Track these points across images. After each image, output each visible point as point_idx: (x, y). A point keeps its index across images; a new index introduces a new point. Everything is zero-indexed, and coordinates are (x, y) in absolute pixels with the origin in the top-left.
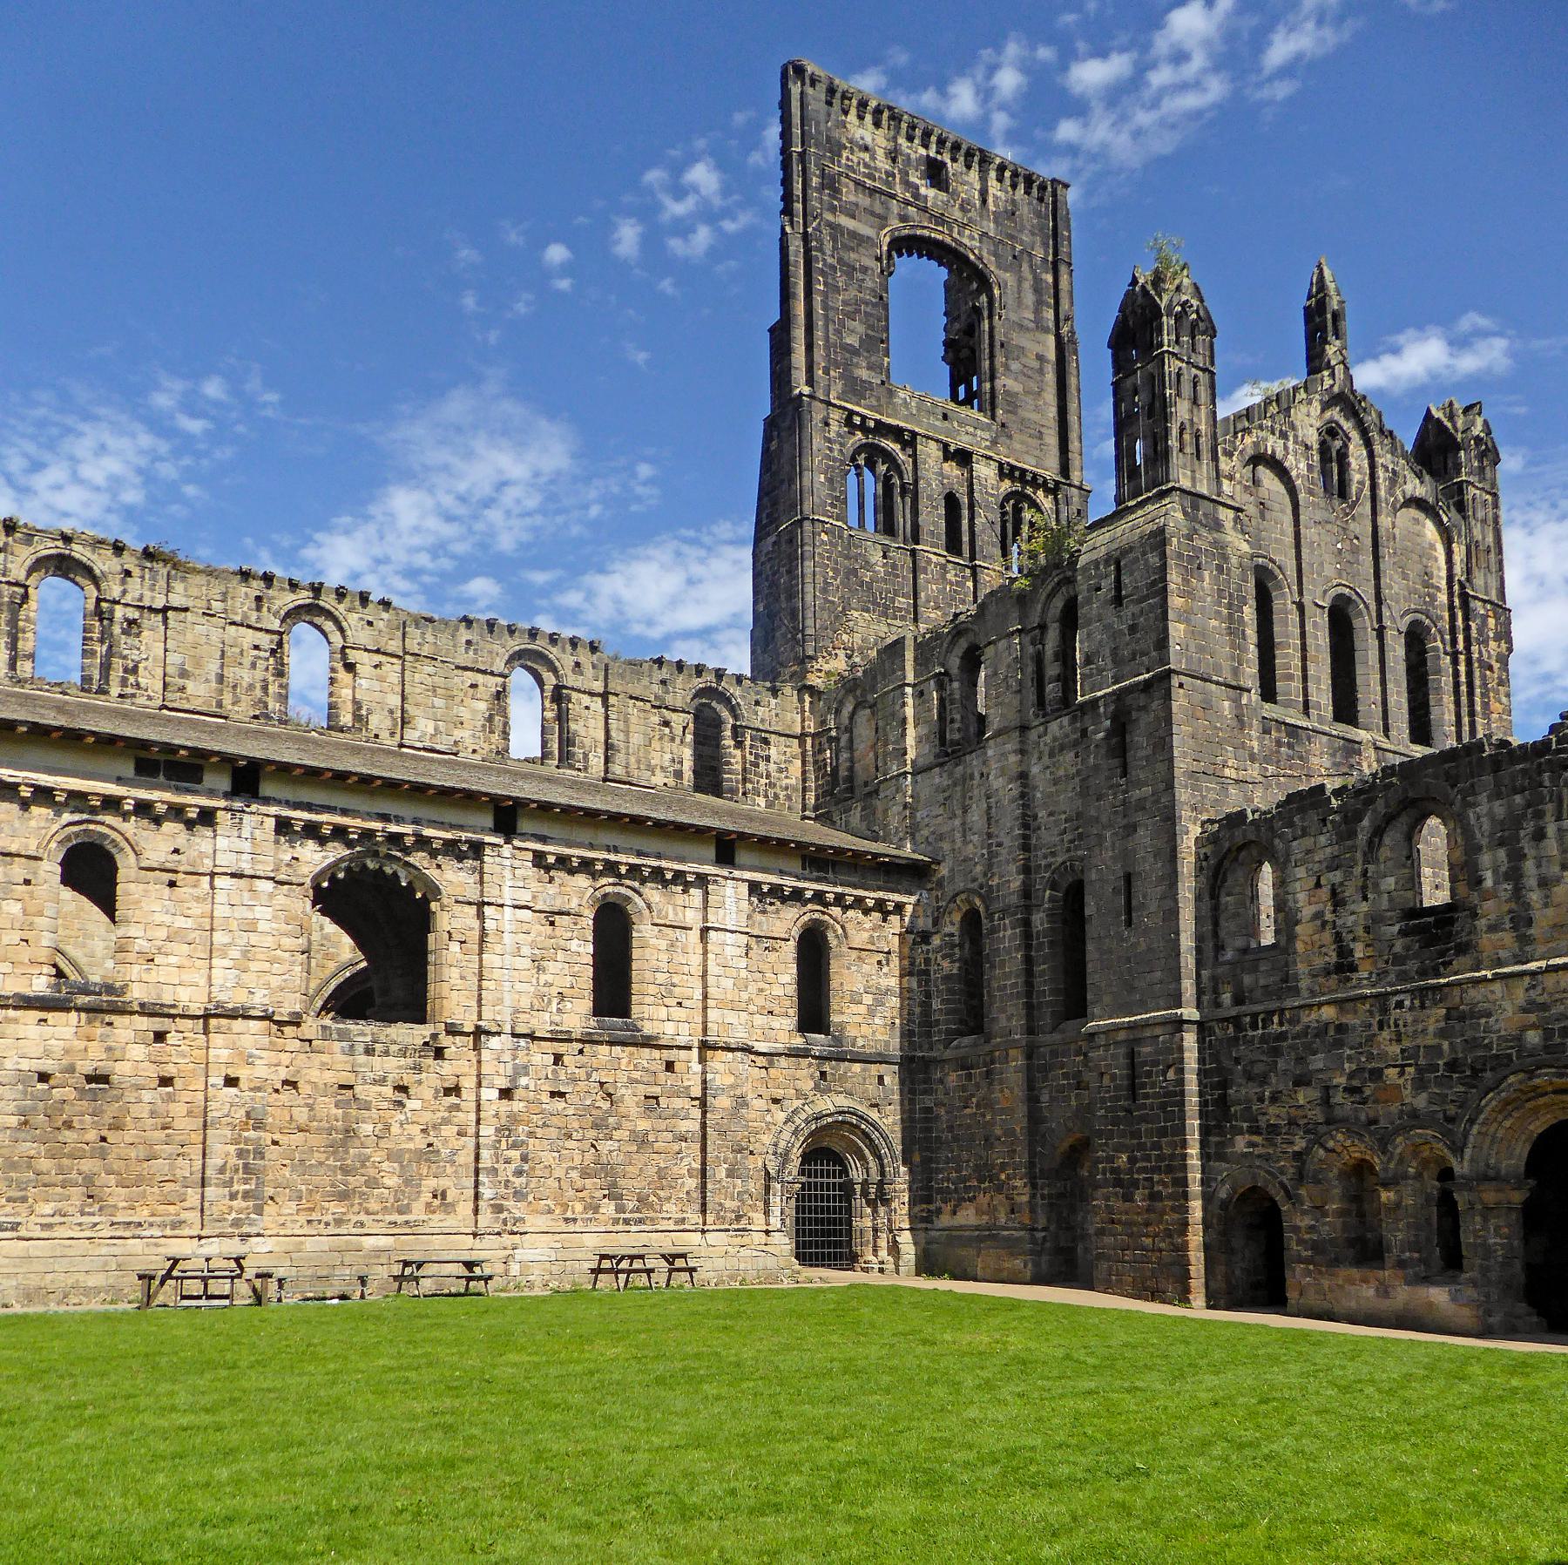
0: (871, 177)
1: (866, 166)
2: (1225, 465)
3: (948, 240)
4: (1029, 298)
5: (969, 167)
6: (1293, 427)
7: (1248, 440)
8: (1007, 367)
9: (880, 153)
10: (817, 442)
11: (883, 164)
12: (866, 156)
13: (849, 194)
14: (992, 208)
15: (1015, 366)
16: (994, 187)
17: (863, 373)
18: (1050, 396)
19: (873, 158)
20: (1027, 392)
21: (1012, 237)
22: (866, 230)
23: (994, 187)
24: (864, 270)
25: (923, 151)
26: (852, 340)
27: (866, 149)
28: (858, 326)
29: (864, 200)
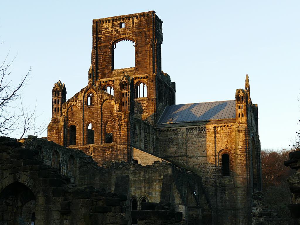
0: (108, 33)
1: (107, 32)
2: (63, 111)
3: (125, 37)
4: (144, 39)
5: (129, 19)
6: (78, 99)
7: (69, 105)
9: (110, 28)
11: (110, 29)
14: (135, 25)
16: (136, 20)
17: (106, 72)
19: (108, 29)
20: (143, 59)
22: (107, 44)
23: (136, 20)
24: (106, 52)
25: (119, 22)
27: (107, 28)
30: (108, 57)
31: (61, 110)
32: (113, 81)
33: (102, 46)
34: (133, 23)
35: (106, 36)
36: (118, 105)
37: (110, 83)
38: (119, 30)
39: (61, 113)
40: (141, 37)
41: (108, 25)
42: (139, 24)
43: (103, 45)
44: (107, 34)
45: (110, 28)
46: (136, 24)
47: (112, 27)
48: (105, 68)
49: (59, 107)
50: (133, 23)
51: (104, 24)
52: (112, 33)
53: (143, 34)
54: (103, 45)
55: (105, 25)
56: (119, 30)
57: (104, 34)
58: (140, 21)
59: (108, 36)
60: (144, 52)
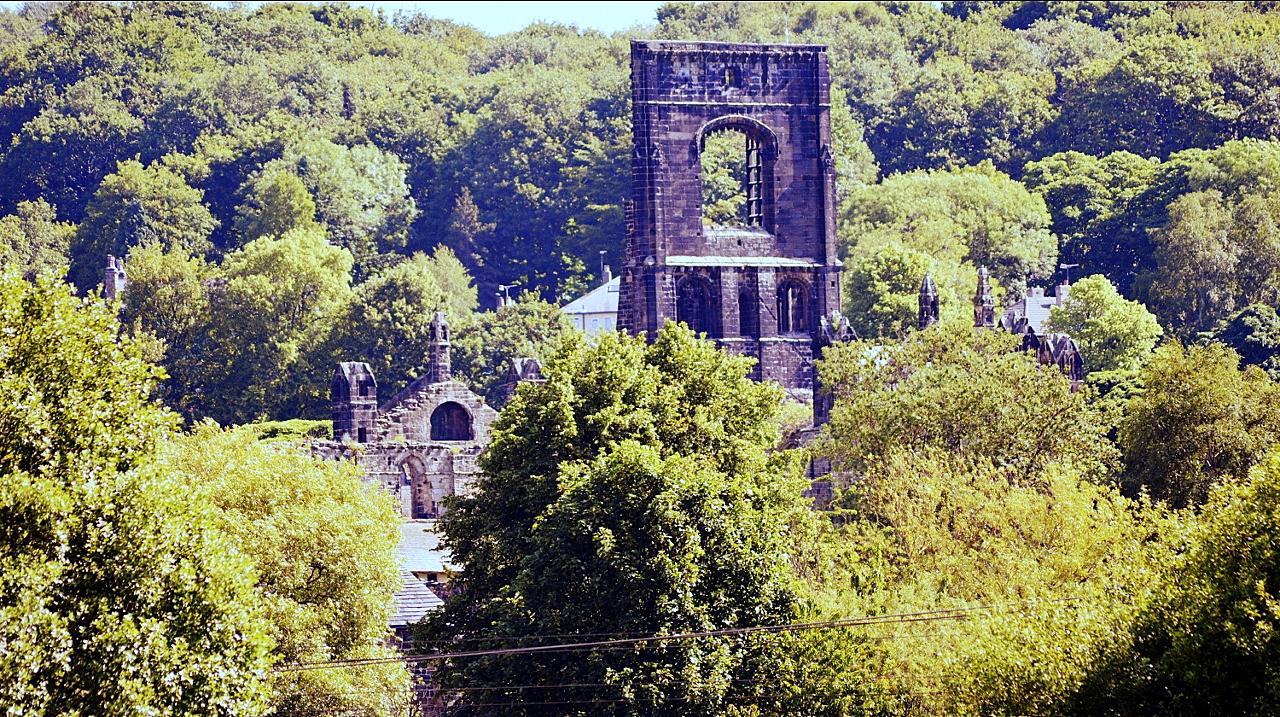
9: (695, 78)
10: (659, 292)
13: (675, 116)
17: (684, 233)
18: (812, 203)
19: (690, 85)
23: (773, 69)
26: (678, 214)
27: (686, 80)
29: (685, 117)
30: (692, 184)
37: (703, 274)
38: (723, 94)
43: (674, 136)
44: (686, 99)
45: (695, 78)
46: (774, 81)
47: (701, 79)
48: (679, 221)
54: (674, 136)
56: (723, 94)
57: (677, 99)
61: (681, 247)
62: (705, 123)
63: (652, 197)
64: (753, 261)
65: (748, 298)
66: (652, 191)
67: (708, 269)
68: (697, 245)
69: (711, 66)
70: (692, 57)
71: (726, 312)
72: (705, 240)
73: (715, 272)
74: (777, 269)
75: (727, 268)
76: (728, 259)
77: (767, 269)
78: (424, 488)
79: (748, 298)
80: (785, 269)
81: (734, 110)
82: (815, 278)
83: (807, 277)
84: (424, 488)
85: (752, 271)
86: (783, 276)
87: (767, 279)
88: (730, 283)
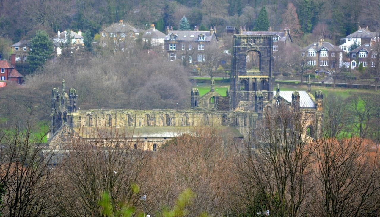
0: (244, 46)
2: (264, 109)
8: (262, 64)
9: (246, 42)
11: (246, 43)
12: (244, 43)
13: (241, 49)
14: (261, 43)
15: (264, 63)
16: (262, 40)
18: (269, 65)
20: (266, 66)
21: (264, 46)
22: (243, 53)
23: (262, 40)
24: (243, 58)
27: (244, 42)
28: (242, 65)
29: (243, 49)
31: (262, 109)
32: (248, 78)
33: (240, 54)
34: (260, 41)
35: (243, 48)
36: (293, 108)
37: (246, 79)
39: (263, 110)
40: (265, 52)
41: (245, 40)
42: (264, 42)
47: (247, 42)
49: (261, 106)
50: (260, 41)
51: (242, 39)
52: (247, 46)
53: (266, 49)
54: (241, 53)
55: (243, 40)
58: (264, 41)
59: (244, 48)
60: (266, 61)
61: (241, 74)
62: (248, 50)
63: (236, 65)
64: (256, 77)
65: (254, 84)
66: (236, 64)
67: (246, 78)
68: (245, 74)
69: (249, 40)
70: (245, 38)
71: (250, 86)
72: (246, 72)
73: (248, 79)
74: (260, 78)
75: (250, 78)
76: (251, 76)
77: (258, 78)
78: (188, 120)
79: (254, 84)
80: (262, 78)
81: (253, 48)
82: (269, 80)
83: (267, 80)
84: (188, 120)
85: (255, 79)
86: (261, 80)
87: (258, 80)
88: (251, 80)
